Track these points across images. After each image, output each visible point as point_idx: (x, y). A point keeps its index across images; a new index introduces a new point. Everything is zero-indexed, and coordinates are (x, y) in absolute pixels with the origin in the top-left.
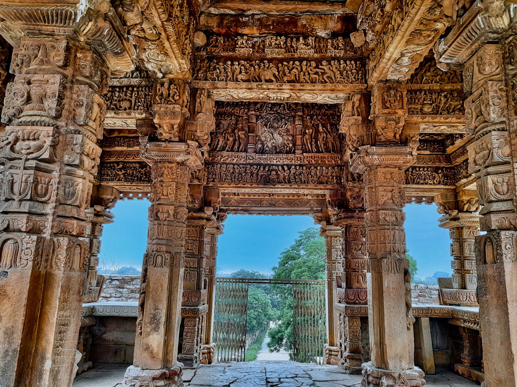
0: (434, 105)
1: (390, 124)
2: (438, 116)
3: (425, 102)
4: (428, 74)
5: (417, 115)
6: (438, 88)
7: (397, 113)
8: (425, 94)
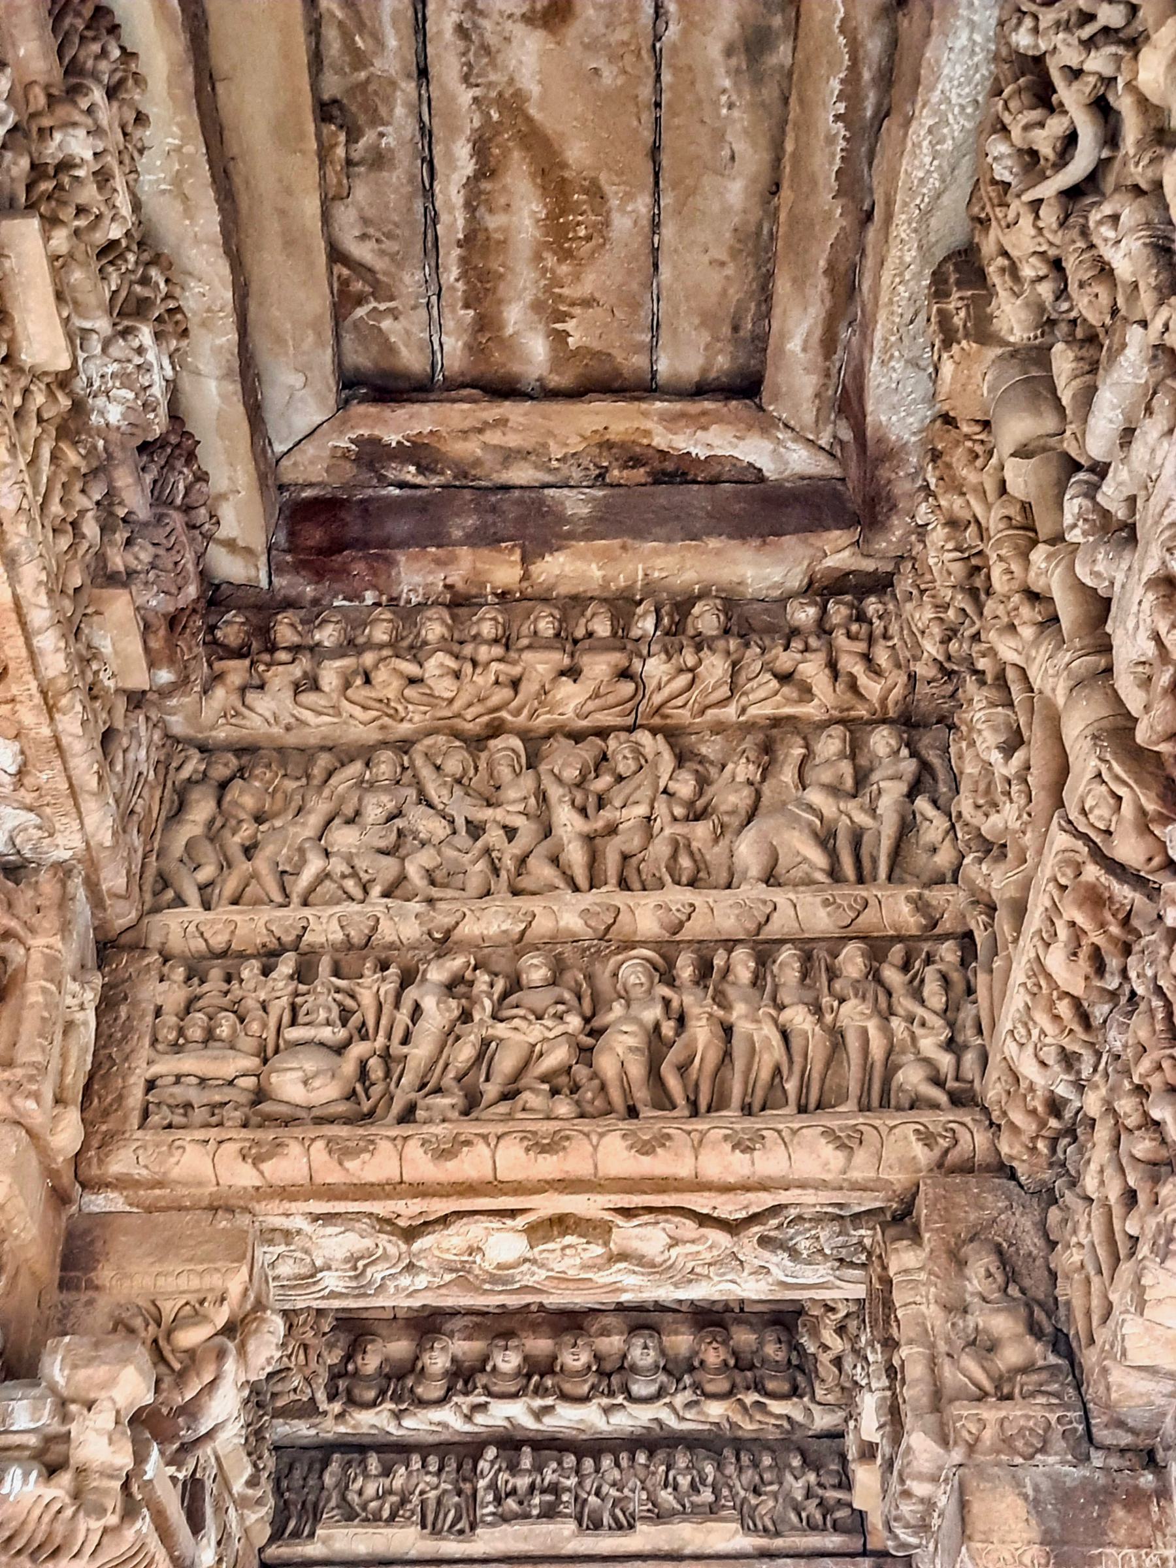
0: (358, 1049)
3: (293, 1034)
4: (344, 838)
5: (213, 1134)
6: (410, 931)
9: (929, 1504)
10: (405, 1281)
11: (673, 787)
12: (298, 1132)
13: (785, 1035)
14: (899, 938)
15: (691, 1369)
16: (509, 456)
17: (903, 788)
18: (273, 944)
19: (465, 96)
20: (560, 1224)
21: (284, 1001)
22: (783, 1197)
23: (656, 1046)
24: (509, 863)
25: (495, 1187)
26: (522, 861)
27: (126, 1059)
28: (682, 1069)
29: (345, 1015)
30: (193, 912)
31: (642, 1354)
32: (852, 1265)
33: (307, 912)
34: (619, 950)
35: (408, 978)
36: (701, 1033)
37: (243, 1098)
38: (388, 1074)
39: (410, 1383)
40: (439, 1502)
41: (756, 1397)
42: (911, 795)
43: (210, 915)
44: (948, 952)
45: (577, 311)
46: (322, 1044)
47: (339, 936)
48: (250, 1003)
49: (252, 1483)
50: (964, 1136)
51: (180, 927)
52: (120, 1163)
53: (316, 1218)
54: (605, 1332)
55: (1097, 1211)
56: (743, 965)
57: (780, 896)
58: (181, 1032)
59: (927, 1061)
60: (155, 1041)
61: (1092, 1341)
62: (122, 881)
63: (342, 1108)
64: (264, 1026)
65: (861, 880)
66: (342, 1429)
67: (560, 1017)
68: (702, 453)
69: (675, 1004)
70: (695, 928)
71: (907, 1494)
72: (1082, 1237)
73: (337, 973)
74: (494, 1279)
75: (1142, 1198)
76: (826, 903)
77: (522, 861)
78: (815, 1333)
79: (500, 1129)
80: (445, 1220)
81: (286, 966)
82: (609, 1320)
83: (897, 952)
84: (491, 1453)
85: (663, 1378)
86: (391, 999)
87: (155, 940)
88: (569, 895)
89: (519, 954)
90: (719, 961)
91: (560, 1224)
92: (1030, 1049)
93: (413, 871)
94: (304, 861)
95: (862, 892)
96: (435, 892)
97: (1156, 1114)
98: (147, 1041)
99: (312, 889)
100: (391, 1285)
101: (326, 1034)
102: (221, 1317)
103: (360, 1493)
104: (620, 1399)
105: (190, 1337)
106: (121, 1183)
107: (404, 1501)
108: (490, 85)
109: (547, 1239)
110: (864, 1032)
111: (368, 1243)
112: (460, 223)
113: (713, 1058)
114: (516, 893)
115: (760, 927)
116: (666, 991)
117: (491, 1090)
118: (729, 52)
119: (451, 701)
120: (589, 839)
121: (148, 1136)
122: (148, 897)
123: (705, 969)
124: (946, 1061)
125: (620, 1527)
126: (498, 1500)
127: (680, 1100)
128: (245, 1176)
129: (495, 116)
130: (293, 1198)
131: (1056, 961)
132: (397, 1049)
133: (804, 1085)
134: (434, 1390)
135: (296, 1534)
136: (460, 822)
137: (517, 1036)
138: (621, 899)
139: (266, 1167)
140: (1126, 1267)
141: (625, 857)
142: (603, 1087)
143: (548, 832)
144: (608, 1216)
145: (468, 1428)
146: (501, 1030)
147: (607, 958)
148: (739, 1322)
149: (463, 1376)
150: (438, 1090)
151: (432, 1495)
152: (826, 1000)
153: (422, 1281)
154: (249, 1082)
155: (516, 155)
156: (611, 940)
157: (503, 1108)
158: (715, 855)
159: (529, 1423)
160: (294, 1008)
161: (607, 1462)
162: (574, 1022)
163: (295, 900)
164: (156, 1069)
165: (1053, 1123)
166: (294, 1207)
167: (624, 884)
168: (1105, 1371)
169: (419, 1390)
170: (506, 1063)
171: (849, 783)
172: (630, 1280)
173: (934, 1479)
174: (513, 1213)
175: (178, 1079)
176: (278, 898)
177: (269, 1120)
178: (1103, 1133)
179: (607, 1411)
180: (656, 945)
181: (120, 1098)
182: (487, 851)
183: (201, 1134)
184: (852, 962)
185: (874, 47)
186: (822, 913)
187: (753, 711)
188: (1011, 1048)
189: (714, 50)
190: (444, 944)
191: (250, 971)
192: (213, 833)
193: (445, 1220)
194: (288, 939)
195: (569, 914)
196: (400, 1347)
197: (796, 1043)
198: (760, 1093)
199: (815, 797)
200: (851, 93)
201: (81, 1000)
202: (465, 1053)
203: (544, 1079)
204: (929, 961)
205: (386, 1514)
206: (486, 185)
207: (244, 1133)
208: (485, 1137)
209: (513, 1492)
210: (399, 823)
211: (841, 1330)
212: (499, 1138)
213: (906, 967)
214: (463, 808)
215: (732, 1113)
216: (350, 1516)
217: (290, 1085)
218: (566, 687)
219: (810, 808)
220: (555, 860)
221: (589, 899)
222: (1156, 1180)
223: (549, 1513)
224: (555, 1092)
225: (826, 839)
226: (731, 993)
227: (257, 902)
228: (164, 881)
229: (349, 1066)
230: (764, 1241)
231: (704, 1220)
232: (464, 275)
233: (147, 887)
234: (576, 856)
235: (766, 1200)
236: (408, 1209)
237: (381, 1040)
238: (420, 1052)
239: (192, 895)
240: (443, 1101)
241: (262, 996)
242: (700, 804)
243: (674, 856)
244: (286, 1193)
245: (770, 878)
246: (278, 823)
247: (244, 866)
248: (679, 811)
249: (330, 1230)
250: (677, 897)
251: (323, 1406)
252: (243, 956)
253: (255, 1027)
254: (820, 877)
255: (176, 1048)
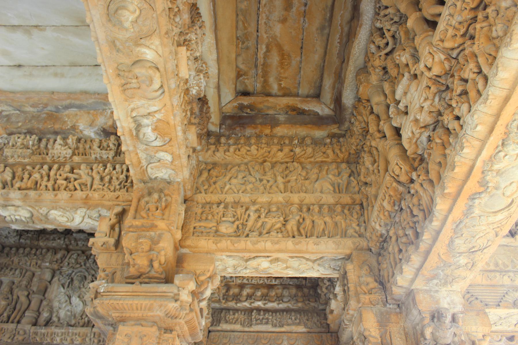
0: (237, 223)
1: (141, 243)
2: (243, 239)
4: (234, 181)
5: (207, 238)
6: (247, 200)
7: (156, 226)
8: (226, 207)
9: (353, 315)
10: (244, 271)
11: (301, 173)
12: (225, 238)
13: (325, 223)
14: (347, 204)
15: (295, 296)
16: (269, 108)
17: (348, 175)
18: (219, 202)
19: (265, 36)
20: (277, 260)
21: (222, 213)
22: (324, 255)
23: (299, 224)
24: (268, 187)
25: (265, 251)
26: (271, 187)
27: (190, 222)
28: (304, 229)
29: (234, 216)
30: (203, 194)
31: (286, 293)
32: (336, 270)
33: (226, 195)
34: (290, 205)
35: (247, 209)
36: (308, 222)
37: (213, 231)
38: (243, 228)
39: (239, 297)
40: (244, 320)
41: (308, 302)
42: (350, 176)
43: (207, 195)
44: (358, 208)
45: (284, 79)
46: (229, 221)
47: (232, 200)
48: (215, 213)
49: (208, 314)
50: (361, 243)
51: (201, 198)
52: (188, 242)
53: (227, 256)
54: (278, 289)
55: (392, 256)
56: (316, 208)
57: (324, 196)
58: (201, 218)
59: (354, 228)
60: (195, 219)
61: (389, 282)
62: (190, 187)
63: (233, 234)
64: (218, 217)
65: (339, 193)
66: (225, 306)
67: (279, 218)
68: (307, 109)
69: (302, 216)
70: (307, 201)
71: (348, 314)
72: (387, 261)
73: (232, 207)
74: (262, 271)
75: (404, 250)
76: (333, 197)
77: (271, 187)
78: (321, 289)
79: (267, 239)
80: (254, 258)
81: (222, 206)
82: (279, 287)
83: (347, 207)
84: (255, 311)
85: (289, 298)
86: (244, 213)
87: (196, 199)
88: (280, 194)
89: (270, 205)
90: (311, 208)
91: (277, 260)
92: (378, 224)
93: (248, 188)
94: (225, 185)
95: (340, 195)
96: (252, 192)
97: (407, 233)
98: (194, 219)
99: (227, 191)
100: (241, 272)
101: (230, 219)
102: (208, 275)
103: (229, 318)
104: (281, 302)
105: (202, 278)
106: (189, 247)
107: (237, 320)
108: (270, 34)
109: (274, 263)
110: (341, 222)
111: (237, 262)
112: (262, 61)
113: (310, 227)
114: (269, 193)
115: (319, 201)
116: (300, 213)
117: (265, 232)
118: (317, 29)
119: (256, 155)
120: (284, 183)
121: (194, 237)
122: (194, 191)
123: (309, 209)
124: (357, 228)
125: (280, 326)
126: (256, 320)
127: (304, 235)
128: (214, 247)
129: (271, 40)
130: (223, 252)
131: (385, 204)
132: (245, 223)
133: (329, 233)
134: (244, 299)
135: (216, 325)
136: (258, 179)
137: (270, 221)
138: (291, 195)
139: (219, 245)
140: (398, 265)
141: (292, 187)
142: (288, 232)
143: (276, 181)
144: (288, 258)
145: (250, 306)
146: (266, 220)
147: (288, 207)
148: (305, 287)
149: (249, 297)
150: (253, 231)
151: (243, 319)
152: (333, 216)
153: (248, 271)
154: (214, 228)
155: (274, 48)
156: (289, 203)
157: (267, 235)
158: (309, 187)
159: (262, 306)
160: (224, 214)
161: (278, 314)
162: (282, 219)
163: (224, 193)
164: (196, 225)
165: (381, 239)
166: (223, 253)
167: (291, 192)
168: (391, 288)
169: (241, 299)
170: (268, 226)
171: (337, 174)
172: (290, 272)
173: (355, 310)
174: (268, 257)
175: (200, 227)
176: (220, 192)
177: (219, 236)
178: (394, 239)
179: (278, 304)
180: (298, 204)
181: (189, 230)
182: (263, 185)
183: (205, 238)
184: (339, 208)
185: (346, 29)
186: (332, 199)
187: (317, 160)
188: (373, 224)
189: (314, 29)
190: (254, 203)
191: (215, 206)
192: (207, 180)
193: (254, 258)
194: (223, 200)
195: (280, 198)
196: (237, 290)
197: (327, 224)
198: (320, 234)
199: (330, 176)
200: (341, 38)
201: (182, 209)
202: (259, 224)
203: (275, 230)
204: (353, 209)
205: (234, 322)
206: (268, 54)
207: (213, 238)
208: (263, 241)
209: (259, 319)
210: (245, 179)
211: (327, 288)
212: (266, 241)
213: (349, 210)
214: (258, 176)
215: (314, 237)
216: (227, 322)
217: (224, 229)
218: (280, 153)
219: (329, 178)
220: (277, 187)
221: (284, 195)
222: (407, 247)
223: (267, 323)
224: (277, 232)
225: (333, 185)
226: (314, 214)
227: (216, 193)
228: (197, 188)
229: (235, 226)
230: (319, 265)
231: (307, 259)
232: (262, 71)
233: (194, 189)
234: (282, 186)
235: (321, 255)
236: (247, 255)
237: (242, 221)
238: (250, 224)
239: (203, 191)
240: (254, 233)
241: (217, 211)
242: (307, 177)
243: (302, 187)
244: (222, 251)
245: (321, 192)
246: (220, 178)
247: (214, 186)
248: (303, 178)
249: (231, 259)
250: (303, 195)
251: (222, 301)
252: (213, 204)
253: (216, 217)
254: (332, 192)
255: (200, 221)
